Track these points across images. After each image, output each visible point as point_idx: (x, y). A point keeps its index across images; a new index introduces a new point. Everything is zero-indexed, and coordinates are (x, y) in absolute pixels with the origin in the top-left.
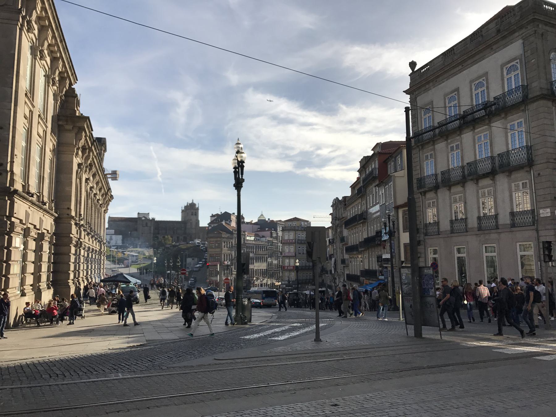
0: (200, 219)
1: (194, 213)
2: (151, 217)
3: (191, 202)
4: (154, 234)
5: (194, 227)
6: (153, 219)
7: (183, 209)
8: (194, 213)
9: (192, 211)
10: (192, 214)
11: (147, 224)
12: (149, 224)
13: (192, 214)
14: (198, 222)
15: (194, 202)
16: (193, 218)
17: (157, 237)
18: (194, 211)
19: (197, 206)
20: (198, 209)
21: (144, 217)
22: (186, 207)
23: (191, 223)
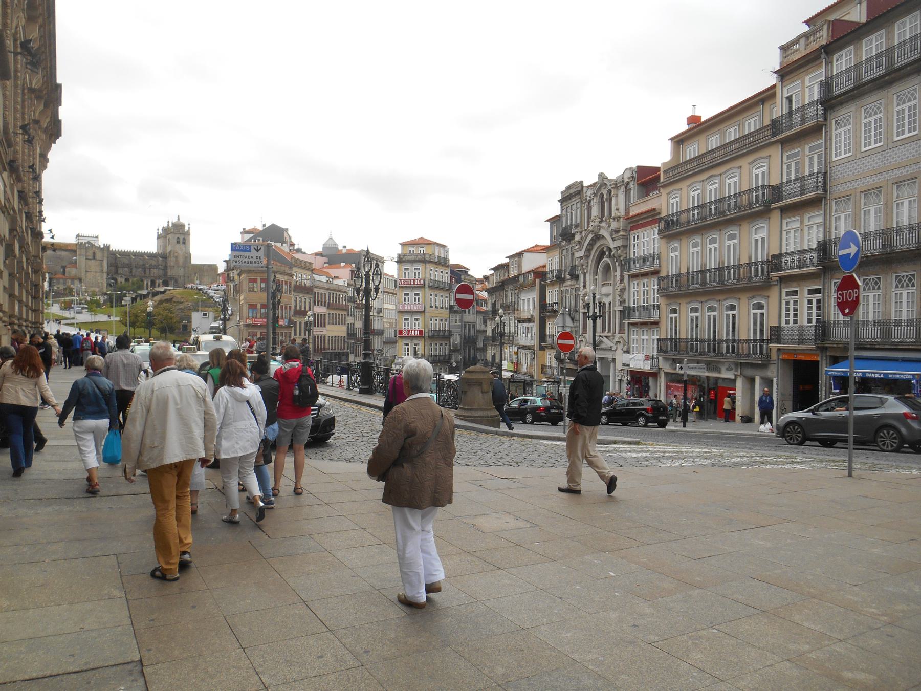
2: (101, 243)
3: (175, 220)
4: (108, 275)
5: (181, 264)
6: (107, 247)
7: (160, 232)
9: (177, 236)
10: (178, 242)
11: (94, 254)
12: (99, 255)
13: (178, 242)
14: (188, 257)
15: (182, 220)
16: (179, 249)
17: (115, 280)
18: (181, 237)
19: (186, 228)
20: (188, 233)
21: (89, 243)
22: (164, 230)
23: (176, 257)
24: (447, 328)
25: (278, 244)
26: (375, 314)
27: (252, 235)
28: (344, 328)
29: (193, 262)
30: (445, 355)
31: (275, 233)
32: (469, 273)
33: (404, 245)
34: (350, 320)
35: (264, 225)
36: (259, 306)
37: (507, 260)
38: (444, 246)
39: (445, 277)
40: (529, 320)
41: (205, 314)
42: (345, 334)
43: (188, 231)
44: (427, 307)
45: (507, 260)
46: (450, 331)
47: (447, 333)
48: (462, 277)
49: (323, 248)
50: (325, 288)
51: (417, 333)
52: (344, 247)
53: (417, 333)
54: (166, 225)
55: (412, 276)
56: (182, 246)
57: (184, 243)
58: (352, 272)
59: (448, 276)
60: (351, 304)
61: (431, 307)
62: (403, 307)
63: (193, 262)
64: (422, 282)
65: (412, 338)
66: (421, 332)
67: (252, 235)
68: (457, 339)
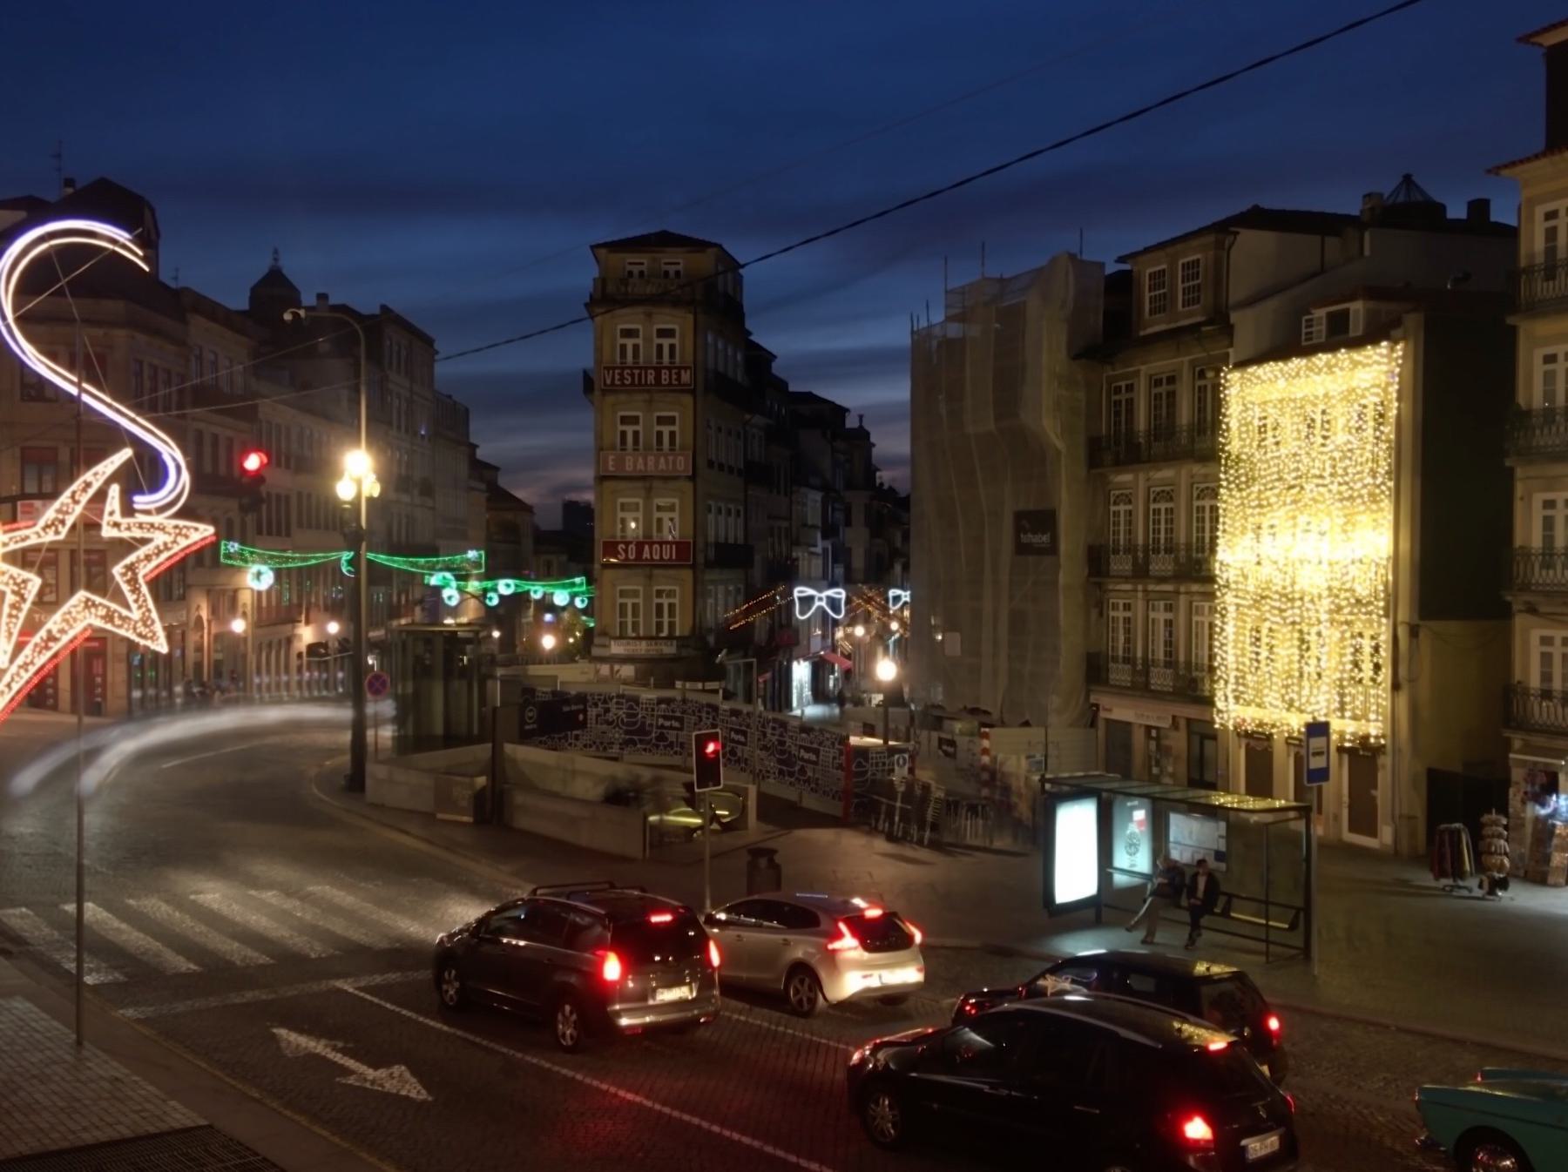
35: (69, 182)
44: (701, 462)
49: (252, 299)
51: (668, 553)
52: (322, 297)
53: (668, 553)
55: (647, 355)
61: (711, 464)
62: (620, 462)
64: (686, 377)
66: (681, 546)
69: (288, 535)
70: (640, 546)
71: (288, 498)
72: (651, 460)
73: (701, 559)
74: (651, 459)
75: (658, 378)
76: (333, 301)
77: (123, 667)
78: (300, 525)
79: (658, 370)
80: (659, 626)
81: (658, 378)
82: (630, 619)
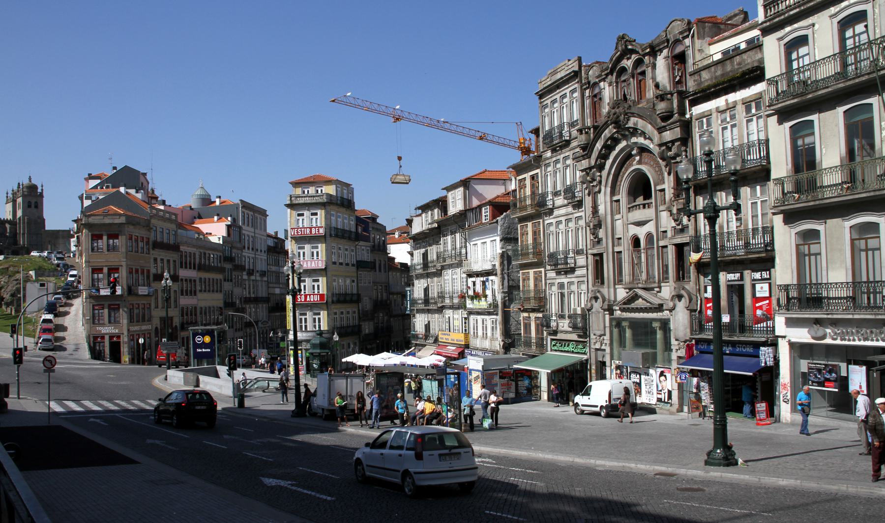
0: (45, 216)
1: (33, 206)
3: (26, 182)
7: (10, 195)
8: (33, 206)
10: (29, 206)
15: (33, 182)
18: (33, 202)
19: (39, 190)
24: (355, 292)
25: (132, 191)
26: (258, 278)
27: (99, 181)
28: (220, 296)
29: (47, 229)
30: (354, 326)
31: (129, 176)
32: (378, 221)
33: (296, 184)
34: (227, 286)
35: (115, 168)
36: (105, 270)
37: (444, 193)
38: (348, 185)
39: (349, 224)
40: (488, 273)
41: (42, 285)
42: (221, 304)
43: (41, 194)
45: (444, 193)
46: (358, 295)
47: (355, 298)
48: (371, 225)
50: (194, 246)
51: (316, 298)
53: (316, 298)
54: (16, 188)
56: (35, 210)
57: (36, 207)
58: (228, 227)
59: (353, 223)
60: (228, 266)
63: (47, 229)
64: (322, 231)
65: (312, 306)
66: (322, 296)
67: (99, 181)
68: (367, 304)
69: (195, 294)
70: (306, 296)
71: (195, 281)
72: (309, 263)
73: (330, 300)
74: (309, 263)
75: (311, 232)
76: (222, 199)
77: (126, 345)
78: (201, 291)
79: (311, 228)
80: (315, 326)
81: (311, 232)
82: (303, 324)
